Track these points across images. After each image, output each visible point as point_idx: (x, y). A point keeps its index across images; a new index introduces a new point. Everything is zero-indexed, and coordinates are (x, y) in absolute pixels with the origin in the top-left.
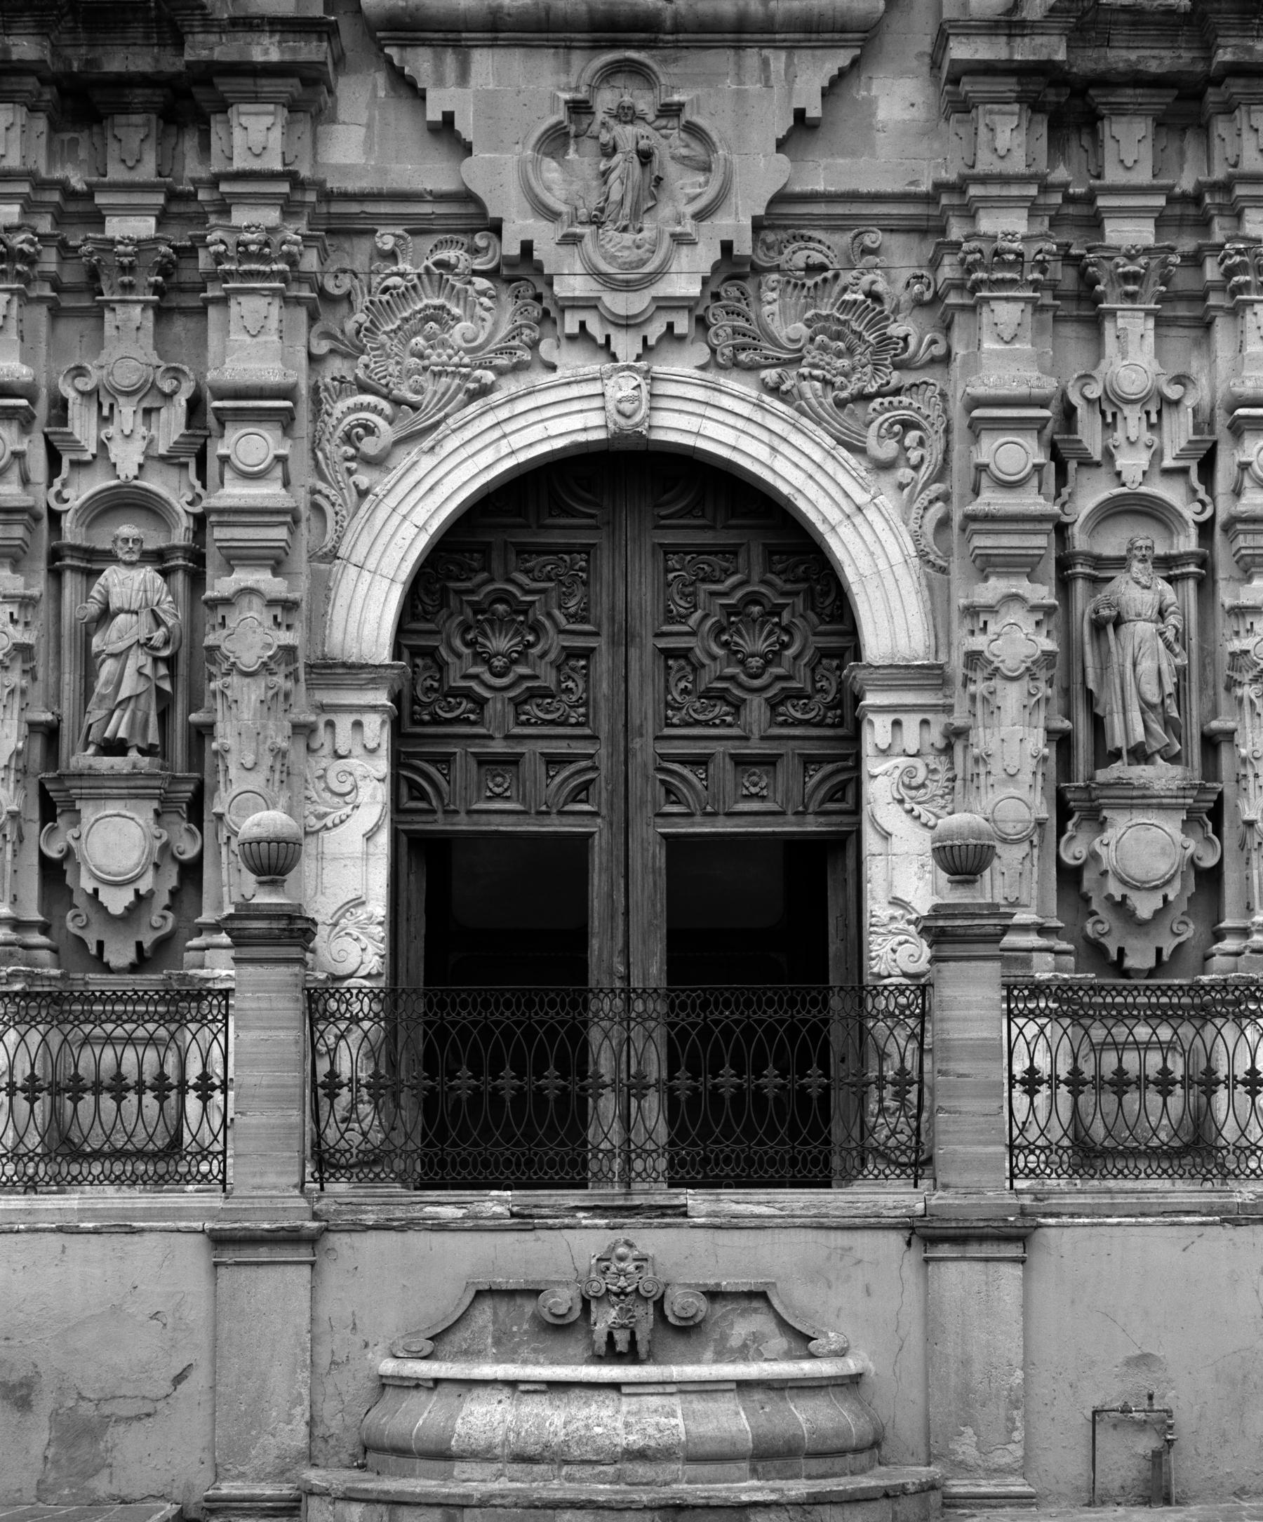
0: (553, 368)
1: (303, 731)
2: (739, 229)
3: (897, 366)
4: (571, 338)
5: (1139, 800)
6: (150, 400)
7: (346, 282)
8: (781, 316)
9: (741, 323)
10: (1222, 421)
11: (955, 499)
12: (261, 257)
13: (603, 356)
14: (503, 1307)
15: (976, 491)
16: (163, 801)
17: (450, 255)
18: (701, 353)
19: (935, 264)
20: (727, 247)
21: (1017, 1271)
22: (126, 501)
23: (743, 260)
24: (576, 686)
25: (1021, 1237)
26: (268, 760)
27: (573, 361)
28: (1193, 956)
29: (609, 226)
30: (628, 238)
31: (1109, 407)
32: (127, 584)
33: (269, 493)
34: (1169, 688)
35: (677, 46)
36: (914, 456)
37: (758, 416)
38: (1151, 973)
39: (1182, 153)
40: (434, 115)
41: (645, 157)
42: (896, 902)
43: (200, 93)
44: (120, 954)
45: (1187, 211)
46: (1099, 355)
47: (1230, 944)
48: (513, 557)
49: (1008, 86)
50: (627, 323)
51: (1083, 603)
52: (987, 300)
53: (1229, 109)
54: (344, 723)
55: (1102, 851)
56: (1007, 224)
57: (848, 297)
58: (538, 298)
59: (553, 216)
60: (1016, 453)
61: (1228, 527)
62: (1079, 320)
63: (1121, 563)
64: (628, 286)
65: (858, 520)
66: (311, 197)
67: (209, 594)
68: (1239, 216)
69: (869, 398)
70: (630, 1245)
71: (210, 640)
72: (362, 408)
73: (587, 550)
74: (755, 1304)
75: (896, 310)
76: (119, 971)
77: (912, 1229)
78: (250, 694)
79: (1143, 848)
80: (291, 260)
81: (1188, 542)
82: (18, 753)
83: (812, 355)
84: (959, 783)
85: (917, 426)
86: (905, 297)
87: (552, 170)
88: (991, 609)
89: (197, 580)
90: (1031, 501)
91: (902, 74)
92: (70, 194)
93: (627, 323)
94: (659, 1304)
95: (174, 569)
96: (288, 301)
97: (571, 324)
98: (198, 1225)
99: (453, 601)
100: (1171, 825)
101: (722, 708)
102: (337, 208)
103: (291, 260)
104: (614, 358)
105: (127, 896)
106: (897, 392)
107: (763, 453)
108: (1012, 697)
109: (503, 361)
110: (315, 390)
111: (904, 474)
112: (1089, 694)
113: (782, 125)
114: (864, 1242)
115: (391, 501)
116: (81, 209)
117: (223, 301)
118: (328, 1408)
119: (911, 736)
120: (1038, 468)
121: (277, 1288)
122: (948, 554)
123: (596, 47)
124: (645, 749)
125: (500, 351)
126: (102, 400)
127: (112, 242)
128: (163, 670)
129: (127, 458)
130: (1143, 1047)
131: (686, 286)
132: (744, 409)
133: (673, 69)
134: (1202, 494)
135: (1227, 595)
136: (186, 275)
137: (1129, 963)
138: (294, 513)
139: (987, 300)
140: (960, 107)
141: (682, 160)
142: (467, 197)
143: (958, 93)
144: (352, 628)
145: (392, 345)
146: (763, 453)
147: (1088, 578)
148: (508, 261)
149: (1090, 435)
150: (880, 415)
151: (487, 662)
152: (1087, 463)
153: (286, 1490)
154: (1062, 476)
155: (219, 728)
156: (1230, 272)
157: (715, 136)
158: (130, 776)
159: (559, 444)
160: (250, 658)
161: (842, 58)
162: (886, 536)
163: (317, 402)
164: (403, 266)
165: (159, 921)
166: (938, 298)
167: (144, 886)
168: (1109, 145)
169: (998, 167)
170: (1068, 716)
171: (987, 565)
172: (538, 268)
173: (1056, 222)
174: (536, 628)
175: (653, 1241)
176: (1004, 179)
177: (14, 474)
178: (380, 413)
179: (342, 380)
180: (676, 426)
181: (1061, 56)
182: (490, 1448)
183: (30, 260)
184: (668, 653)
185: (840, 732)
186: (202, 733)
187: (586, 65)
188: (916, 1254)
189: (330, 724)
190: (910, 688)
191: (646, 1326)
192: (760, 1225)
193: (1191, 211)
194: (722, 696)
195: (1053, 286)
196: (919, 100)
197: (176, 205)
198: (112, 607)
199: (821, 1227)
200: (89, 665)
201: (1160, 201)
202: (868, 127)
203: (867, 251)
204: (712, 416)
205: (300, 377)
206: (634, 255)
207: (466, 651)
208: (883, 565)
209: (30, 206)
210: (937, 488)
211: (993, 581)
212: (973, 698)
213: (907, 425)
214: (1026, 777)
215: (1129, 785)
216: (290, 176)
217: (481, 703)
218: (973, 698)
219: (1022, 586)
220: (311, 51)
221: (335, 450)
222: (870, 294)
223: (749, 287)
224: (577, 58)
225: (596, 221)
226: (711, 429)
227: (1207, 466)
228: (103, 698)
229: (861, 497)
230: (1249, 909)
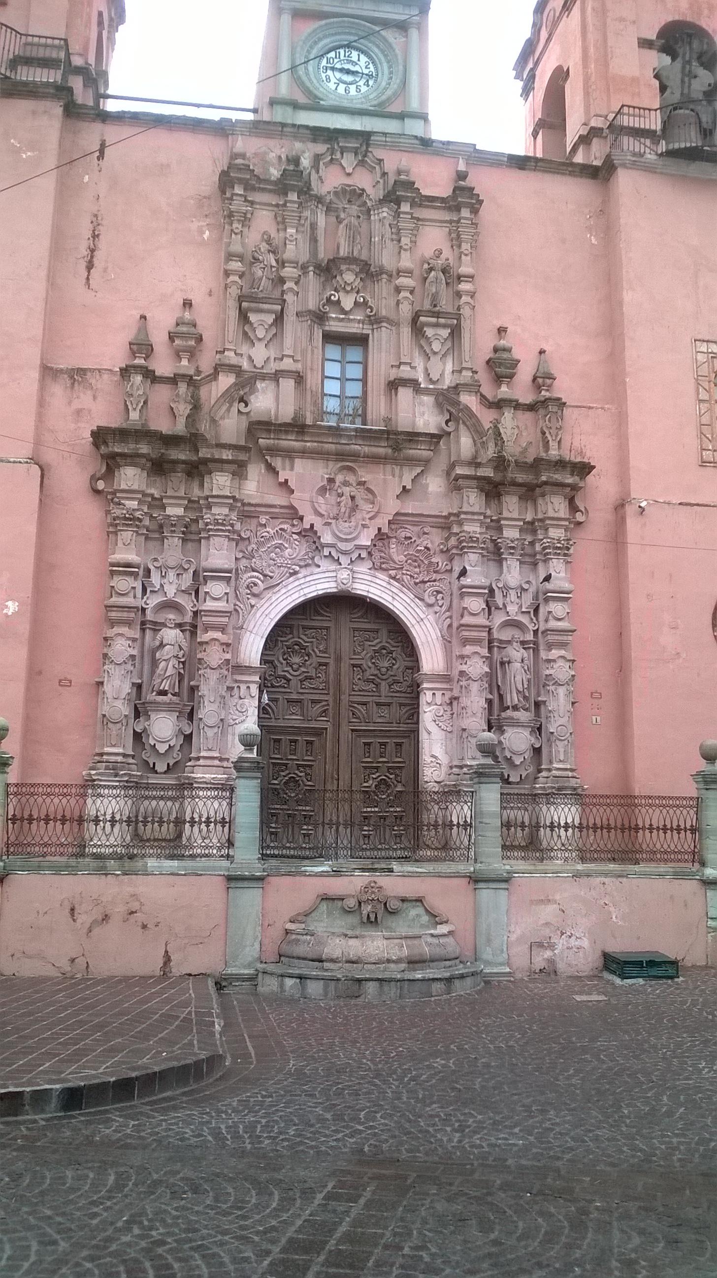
0: (319, 566)
1: (231, 689)
2: (384, 524)
3: (435, 572)
4: (325, 556)
6: (181, 570)
7: (248, 533)
8: (396, 553)
9: (383, 555)
10: (541, 597)
11: (454, 618)
12: (223, 525)
13: (336, 564)
14: (330, 903)
15: (462, 616)
16: (180, 712)
17: (285, 526)
19: (447, 539)
20: (379, 529)
21: (506, 893)
22: (170, 605)
23: (384, 534)
24: (322, 676)
25: (506, 881)
26: (219, 699)
27: (325, 564)
28: (532, 778)
29: (340, 520)
30: (347, 524)
31: (506, 589)
32: (171, 635)
33: (220, 605)
34: (526, 686)
35: (363, 462)
36: (440, 603)
37: (388, 587)
38: (518, 783)
39: (527, 508)
40: (281, 480)
41: (353, 498)
42: (433, 756)
43: (201, 468)
44: (161, 767)
45: (530, 527)
46: (501, 573)
47: (544, 774)
48: (301, 630)
49: (474, 483)
51: (496, 655)
52: (467, 552)
53: (543, 495)
54: (243, 687)
55: (503, 741)
56: (473, 528)
57: (419, 548)
58: (314, 542)
59: (322, 515)
60: (476, 604)
61: (543, 633)
62: (494, 560)
63: (509, 642)
64: (346, 540)
65: (421, 623)
66: (239, 504)
67: (199, 640)
68: (547, 530)
69: (426, 582)
70: (375, 883)
71: (199, 656)
72: (253, 577)
73: (327, 628)
74: (418, 904)
75: (434, 554)
76: (161, 773)
77: (470, 877)
78: (213, 676)
79: (518, 740)
81: (530, 637)
82: (129, 694)
83: (408, 567)
84: (455, 715)
85: (441, 593)
86: (437, 549)
87: (321, 500)
88: (468, 657)
89: (193, 634)
90: (482, 620)
91: (437, 476)
92: (154, 498)
94: (385, 904)
95: (186, 630)
96: (230, 539)
97: (326, 552)
98: (222, 873)
99: (280, 644)
100: (526, 733)
102: (246, 508)
103: (232, 525)
104: (340, 564)
106: (435, 581)
107: (390, 599)
108: (475, 687)
109: (302, 563)
110: (237, 570)
111: (437, 608)
112: (498, 686)
114: (456, 881)
115: (262, 609)
116: (158, 503)
117: (208, 538)
118: (266, 941)
119: (439, 699)
120: (483, 609)
121: (250, 897)
122: (451, 636)
123: (337, 460)
124: (345, 698)
125: (300, 560)
126: (163, 570)
127: (169, 516)
128: (181, 666)
129: (171, 591)
131: (365, 540)
132: (385, 584)
133: (362, 469)
134: (535, 620)
135: (543, 655)
136: (193, 528)
137: (511, 780)
138: (230, 612)
139: (467, 552)
140: (459, 489)
141: (366, 500)
142: (292, 507)
143: (455, 484)
144: (248, 653)
145: (264, 556)
146: (390, 599)
147: (498, 647)
148: (305, 530)
149: (499, 599)
150: (430, 589)
151: (291, 666)
152: (497, 608)
153: (252, 971)
154: (490, 614)
155: (202, 687)
156: (544, 548)
157: (376, 492)
158: (169, 704)
159: (320, 592)
160: (214, 664)
161: (419, 470)
162: (431, 630)
163: (237, 574)
164: (268, 529)
165: (176, 756)
166: (448, 550)
168: (504, 504)
169: (470, 510)
170: (491, 693)
171: (465, 642)
172: (316, 533)
173: (487, 528)
174: (308, 655)
175: (383, 881)
176: (473, 513)
177: (132, 594)
178: (257, 578)
179: (246, 567)
181: (492, 475)
182: (337, 958)
183: (140, 520)
184: (354, 666)
185: (412, 695)
187: (333, 466)
188: (472, 886)
189: (239, 687)
190: (438, 682)
191: (376, 913)
192: (419, 875)
193: (530, 527)
195: (487, 549)
196: (443, 485)
197: (192, 504)
198: (164, 643)
199: (440, 876)
200: (154, 663)
201: (522, 523)
202: (426, 492)
203: (425, 533)
205: (233, 566)
206: (347, 530)
207: (284, 662)
208: (429, 639)
209: (140, 502)
210: (448, 614)
211: (468, 647)
212: (461, 687)
213: (438, 592)
215: (513, 719)
216: (234, 498)
217: (289, 680)
218: (461, 687)
219: (477, 649)
220: (242, 457)
221: (244, 591)
222: (426, 548)
223: (386, 542)
224: (331, 464)
225: (336, 518)
226: (372, 590)
227: (536, 611)
228: (160, 675)
229: (422, 616)
230: (551, 762)
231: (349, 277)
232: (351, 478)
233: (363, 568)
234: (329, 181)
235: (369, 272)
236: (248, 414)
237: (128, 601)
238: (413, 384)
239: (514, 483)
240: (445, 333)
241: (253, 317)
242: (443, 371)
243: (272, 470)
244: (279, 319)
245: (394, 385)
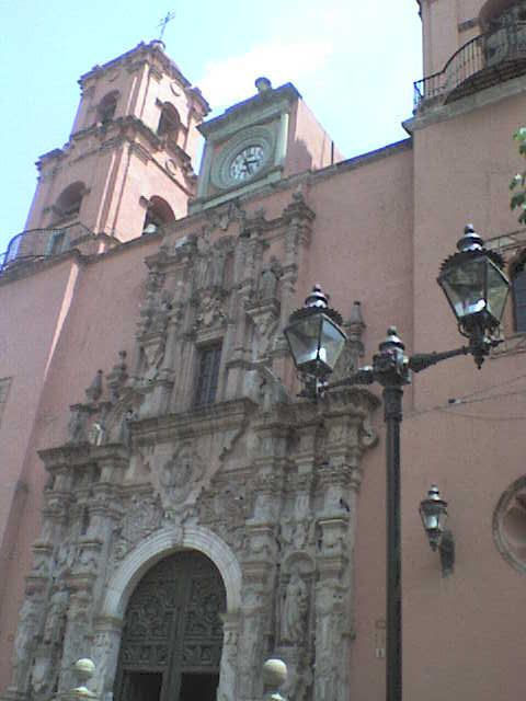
8: (218, 507)
18: (196, 520)
20: (203, 488)
27: (167, 524)
31: (292, 524)
50: (178, 513)
93: (178, 513)
101: (201, 629)
108: (248, 623)
113: (221, 452)
131: (191, 500)
149: (287, 535)
161: (235, 432)
194: (200, 625)
204: (199, 539)
214: (250, 652)
231: (207, 300)
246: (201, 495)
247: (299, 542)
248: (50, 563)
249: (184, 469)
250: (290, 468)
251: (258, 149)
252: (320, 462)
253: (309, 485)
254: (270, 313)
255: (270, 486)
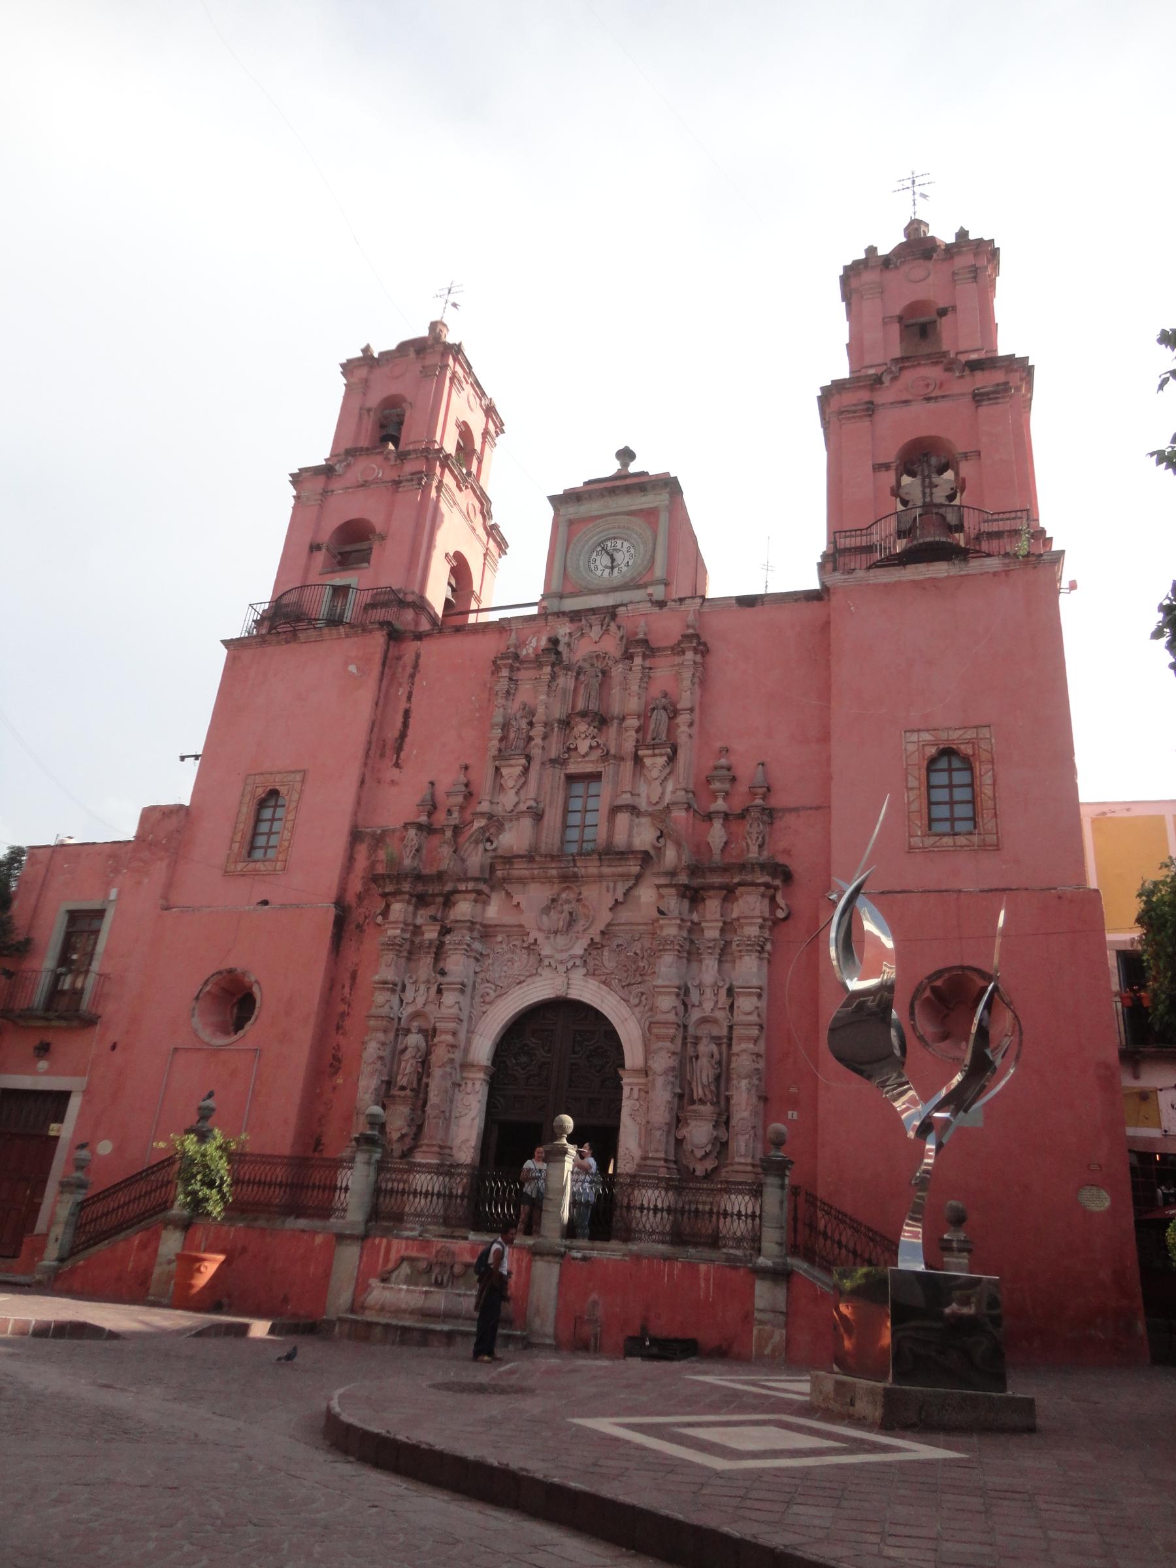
5: (699, 1116)
8: (609, 960)
18: (584, 971)
22: (416, 1015)
27: (546, 972)
32: (414, 1039)
40: (515, 903)
50: (561, 962)
53: (742, 895)
54: (470, 1084)
64: (562, 951)
80: (469, 945)
87: (545, 918)
93: (561, 962)
96: (468, 957)
105: (399, 1135)
107: (599, 1002)
108: (660, 1081)
113: (611, 903)
130: (704, 1203)
131: (578, 950)
142: (521, 926)
148: (531, 944)
149: (694, 997)
150: (636, 989)
161: (631, 883)
167: (404, 1131)
180: (574, 994)
186: (728, 1099)
204: (586, 991)
209: (403, 930)
213: (642, 994)
232: (572, 896)
233: (577, 975)
234: (582, 650)
235: (602, 721)
236: (495, 850)
237: (384, 1011)
238: (634, 810)
239: (712, 887)
240: (661, 760)
241: (504, 771)
242: (663, 794)
243: (508, 894)
244: (526, 770)
245: (615, 810)
246: (589, 945)
247: (708, 1005)
248: (395, 1001)
249: (566, 915)
250: (695, 928)
251: (626, 544)
252: (728, 927)
253: (718, 951)
254: (665, 758)
255: (677, 947)
